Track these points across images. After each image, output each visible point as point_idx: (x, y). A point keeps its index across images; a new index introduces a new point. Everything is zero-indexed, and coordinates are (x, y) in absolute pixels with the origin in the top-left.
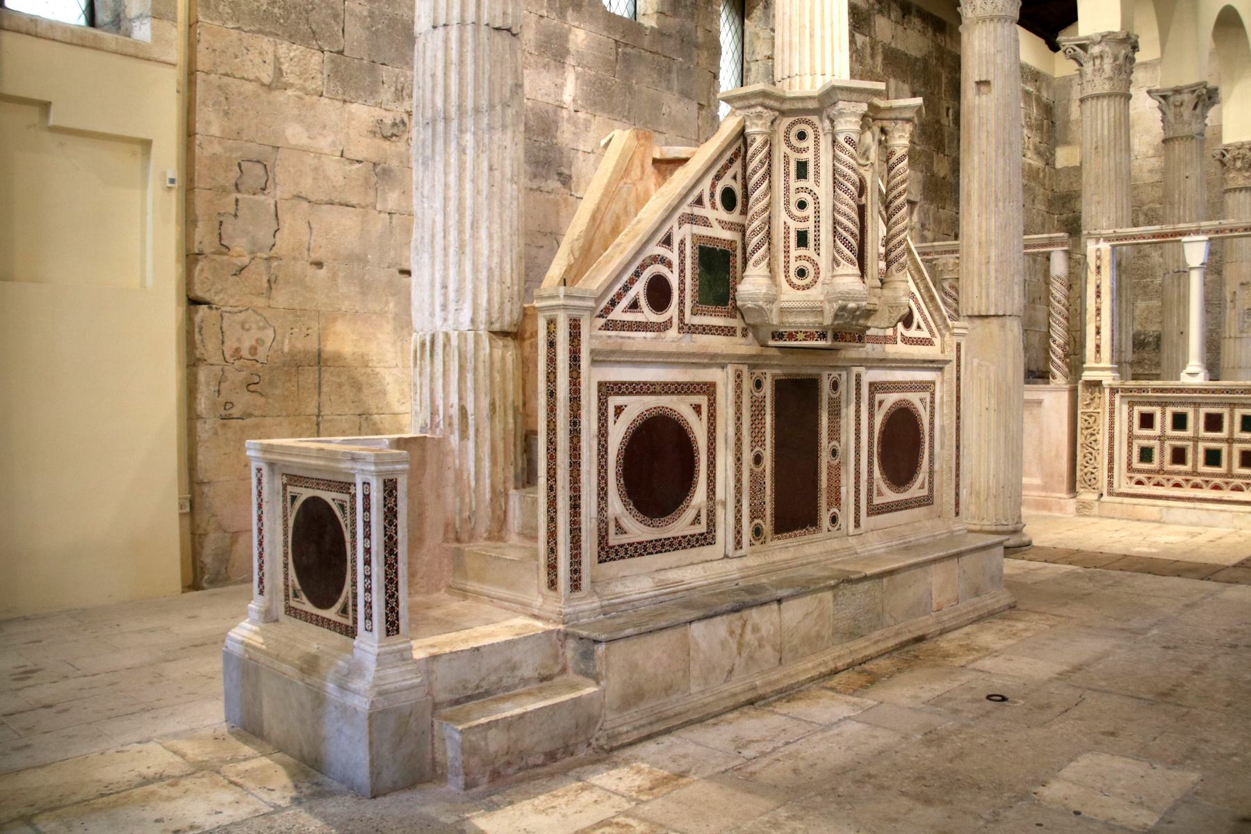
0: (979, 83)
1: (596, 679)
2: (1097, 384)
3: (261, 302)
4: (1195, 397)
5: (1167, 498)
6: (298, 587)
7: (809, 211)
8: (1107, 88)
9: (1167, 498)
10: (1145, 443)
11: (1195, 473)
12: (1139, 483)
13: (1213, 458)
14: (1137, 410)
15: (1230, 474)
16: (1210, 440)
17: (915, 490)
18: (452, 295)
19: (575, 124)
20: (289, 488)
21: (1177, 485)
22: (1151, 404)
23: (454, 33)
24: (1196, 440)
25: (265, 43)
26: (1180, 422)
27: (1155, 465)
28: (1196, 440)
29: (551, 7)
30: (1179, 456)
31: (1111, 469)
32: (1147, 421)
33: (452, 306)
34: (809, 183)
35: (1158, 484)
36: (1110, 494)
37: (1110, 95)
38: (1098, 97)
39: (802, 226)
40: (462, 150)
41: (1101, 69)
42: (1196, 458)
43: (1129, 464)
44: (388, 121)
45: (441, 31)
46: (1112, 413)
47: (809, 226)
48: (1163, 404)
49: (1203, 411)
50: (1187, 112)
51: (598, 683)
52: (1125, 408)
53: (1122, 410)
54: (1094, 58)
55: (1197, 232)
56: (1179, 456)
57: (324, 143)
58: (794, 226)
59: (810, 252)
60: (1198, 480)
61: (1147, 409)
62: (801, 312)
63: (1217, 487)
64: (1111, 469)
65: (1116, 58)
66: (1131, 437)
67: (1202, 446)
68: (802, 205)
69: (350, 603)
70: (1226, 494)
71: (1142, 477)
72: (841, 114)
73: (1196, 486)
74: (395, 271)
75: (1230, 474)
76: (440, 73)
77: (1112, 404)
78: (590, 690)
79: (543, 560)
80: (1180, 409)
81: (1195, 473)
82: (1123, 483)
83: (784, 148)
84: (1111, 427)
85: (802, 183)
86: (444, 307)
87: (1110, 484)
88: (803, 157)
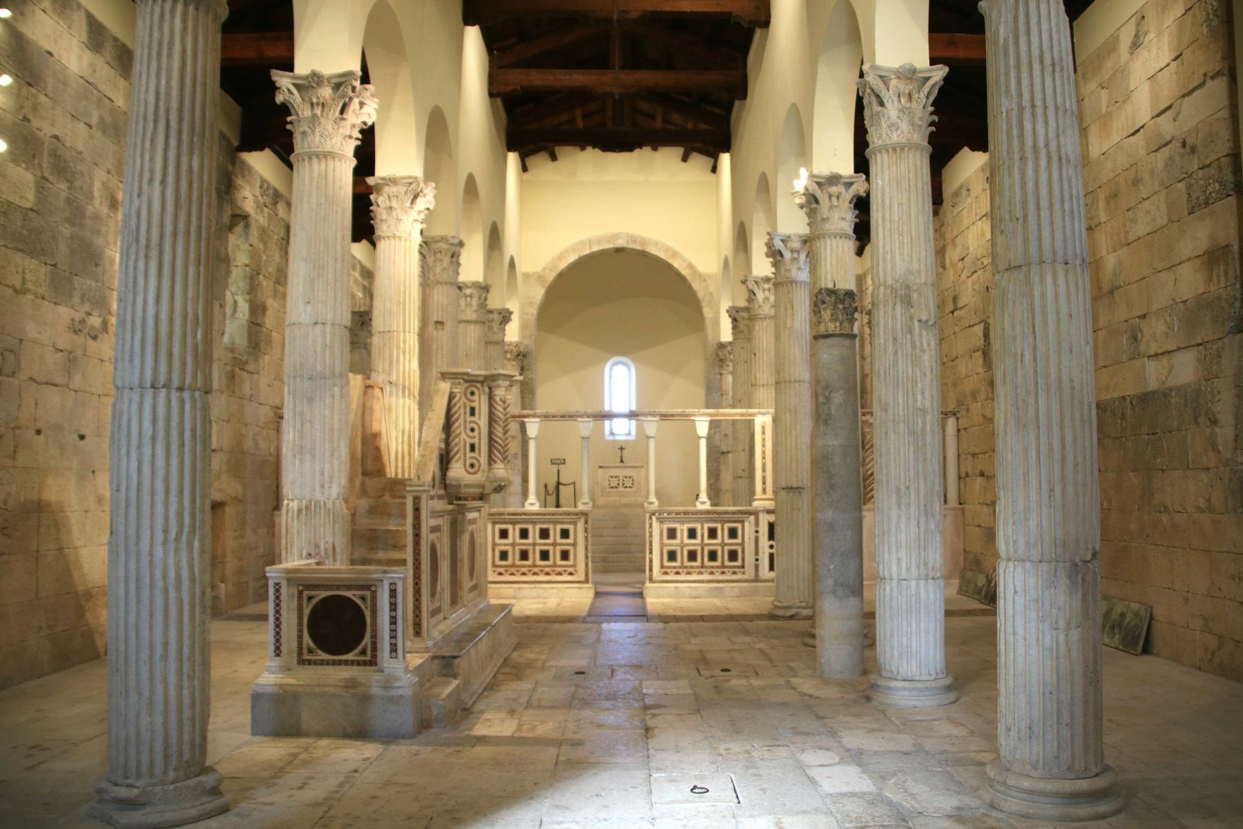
0: (438, 322)
1: (455, 676)
3: (10, 462)
4: (533, 518)
6: (312, 645)
7: (476, 433)
8: (474, 317)
10: (503, 548)
11: (534, 565)
12: (500, 574)
13: (545, 555)
14: (498, 527)
15: (555, 565)
16: (543, 544)
18: (327, 479)
21: (524, 574)
22: (506, 523)
23: (328, 329)
24: (534, 545)
25: (18, 257)
26: (524, 534)
27: (509, 562)
28: (534, 545)
30: (524, 555)
32: (504, 534)
33: (327, 486)
34: (476, 419)
35: (512, 574)
37: (476, 322)
38: (468, 322)
39: (472, 441)
40: (333, 397)
41: (471, 305)
42: (535, 556)
43: (493, 562)
44: (77, 320)
45: (319, 327)
47: (476, 441)
48: (514, 523)
49: (538, 527)
50: (496, 326)
51: (455, 678)
52: (489, 526)
54: (466, 296)
55: (534, 416)
56: (524, 555)
57: (45, 337)
58: (469, 441)
59: (476, 455)
60: (536, 570)
61: (503, 526)
63: (547, 574)
65: (480, 298)
66: (494, 545)
67: (538, 549)
68: (472, 430)
71: (501, 570)
73: (535, 574)
74: (76, 436)
75: (555, 565)
76: (319, 350)
80: (524, 526)
81: (534, 565)
83: (464, 399)
85: (472, 419)
86: (322, 486)
88: (474, 404)
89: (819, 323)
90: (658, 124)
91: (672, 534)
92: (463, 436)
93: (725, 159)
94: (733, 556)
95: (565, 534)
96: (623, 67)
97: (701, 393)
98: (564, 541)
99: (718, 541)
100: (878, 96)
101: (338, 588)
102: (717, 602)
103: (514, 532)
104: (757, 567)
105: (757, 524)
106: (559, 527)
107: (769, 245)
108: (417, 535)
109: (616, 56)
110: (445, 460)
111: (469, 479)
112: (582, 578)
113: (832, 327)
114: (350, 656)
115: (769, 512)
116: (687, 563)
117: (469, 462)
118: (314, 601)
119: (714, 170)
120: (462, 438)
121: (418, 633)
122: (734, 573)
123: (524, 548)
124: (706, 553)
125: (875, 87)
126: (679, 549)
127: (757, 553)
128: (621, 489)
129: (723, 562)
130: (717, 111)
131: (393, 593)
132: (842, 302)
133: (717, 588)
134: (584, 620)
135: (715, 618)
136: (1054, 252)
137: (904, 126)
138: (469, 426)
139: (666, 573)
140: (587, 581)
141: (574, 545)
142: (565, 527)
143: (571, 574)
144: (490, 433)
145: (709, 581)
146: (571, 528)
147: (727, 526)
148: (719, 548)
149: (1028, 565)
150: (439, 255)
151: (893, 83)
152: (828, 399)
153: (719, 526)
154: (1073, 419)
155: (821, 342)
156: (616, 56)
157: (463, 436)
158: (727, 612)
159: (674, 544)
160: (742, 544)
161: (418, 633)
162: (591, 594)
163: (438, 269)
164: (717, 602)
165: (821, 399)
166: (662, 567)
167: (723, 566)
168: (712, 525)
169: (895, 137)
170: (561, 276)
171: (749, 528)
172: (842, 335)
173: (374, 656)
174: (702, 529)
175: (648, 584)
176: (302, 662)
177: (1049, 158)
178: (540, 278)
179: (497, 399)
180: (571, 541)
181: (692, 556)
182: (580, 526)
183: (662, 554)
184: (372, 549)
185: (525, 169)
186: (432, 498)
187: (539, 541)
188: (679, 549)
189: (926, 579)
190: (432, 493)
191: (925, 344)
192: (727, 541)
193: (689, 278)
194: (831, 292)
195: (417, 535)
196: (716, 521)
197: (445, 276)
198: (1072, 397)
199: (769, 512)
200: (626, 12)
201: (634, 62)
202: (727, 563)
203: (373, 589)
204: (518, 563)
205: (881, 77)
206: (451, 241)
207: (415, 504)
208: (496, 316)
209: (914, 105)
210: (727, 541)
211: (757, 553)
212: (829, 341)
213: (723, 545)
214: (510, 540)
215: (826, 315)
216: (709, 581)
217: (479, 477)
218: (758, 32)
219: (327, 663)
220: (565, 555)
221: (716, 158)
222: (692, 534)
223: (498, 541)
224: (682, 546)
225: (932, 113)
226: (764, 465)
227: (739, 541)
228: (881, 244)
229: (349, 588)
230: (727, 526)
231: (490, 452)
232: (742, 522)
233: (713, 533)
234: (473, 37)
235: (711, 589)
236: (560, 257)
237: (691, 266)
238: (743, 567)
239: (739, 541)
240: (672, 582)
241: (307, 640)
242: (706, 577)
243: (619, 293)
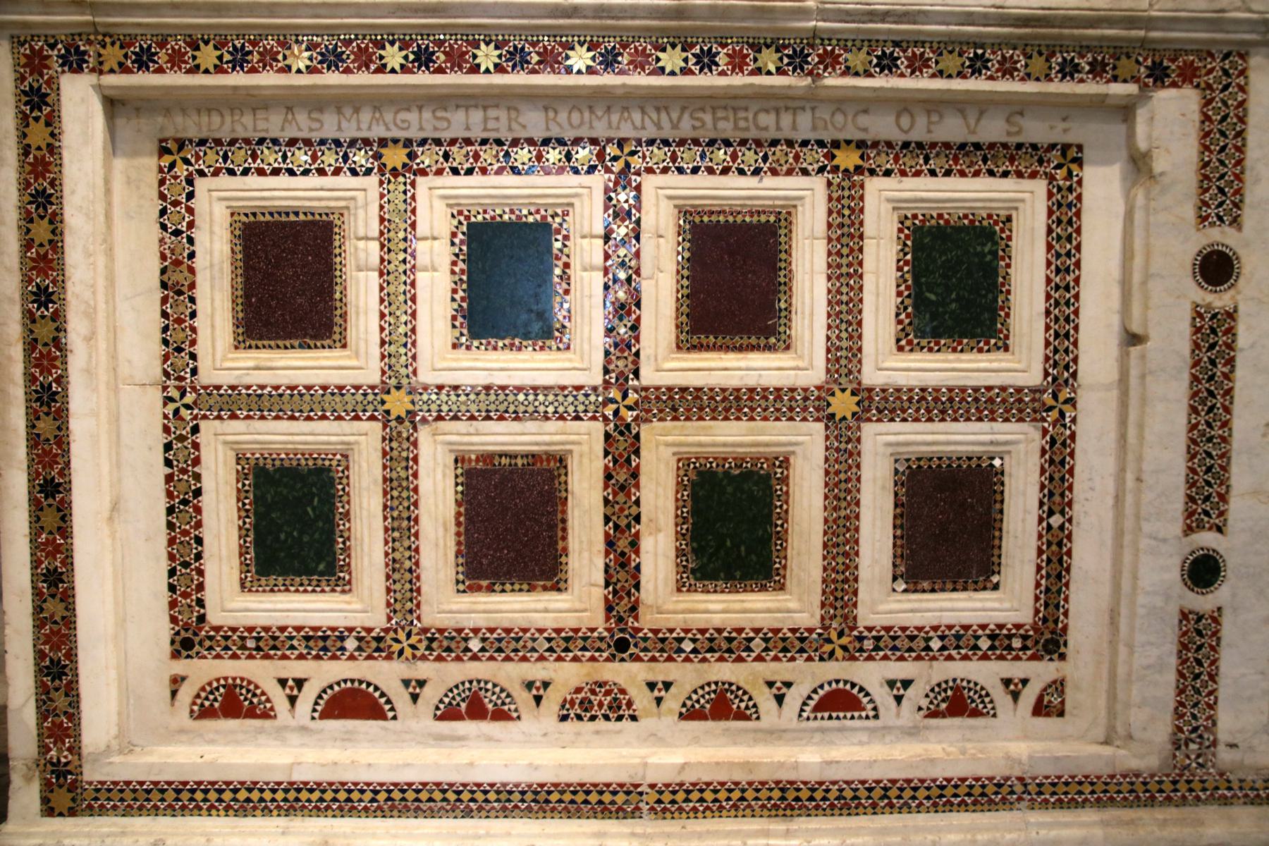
94: (949, 522)
116: (446, 602)
122: (958, 703)
124: (659, 497)
129: (840, 586)
139: (232, 703)
147: (886, 200)
148: (806, 444)
160: (1049, 404)
166: (187, 642)
167: (840, 631)
174: (624, 242)
181: (511, 522)
183: (183, 501)
188: (363, 443)
192: (887, 363)
196: (775, 153)
202: (883, 602)
210: (887, 363)
227: (1019, 363)
232: (1060, 164)
238: (1047, 637)
239: (1019, 363)
242: (663, 749)
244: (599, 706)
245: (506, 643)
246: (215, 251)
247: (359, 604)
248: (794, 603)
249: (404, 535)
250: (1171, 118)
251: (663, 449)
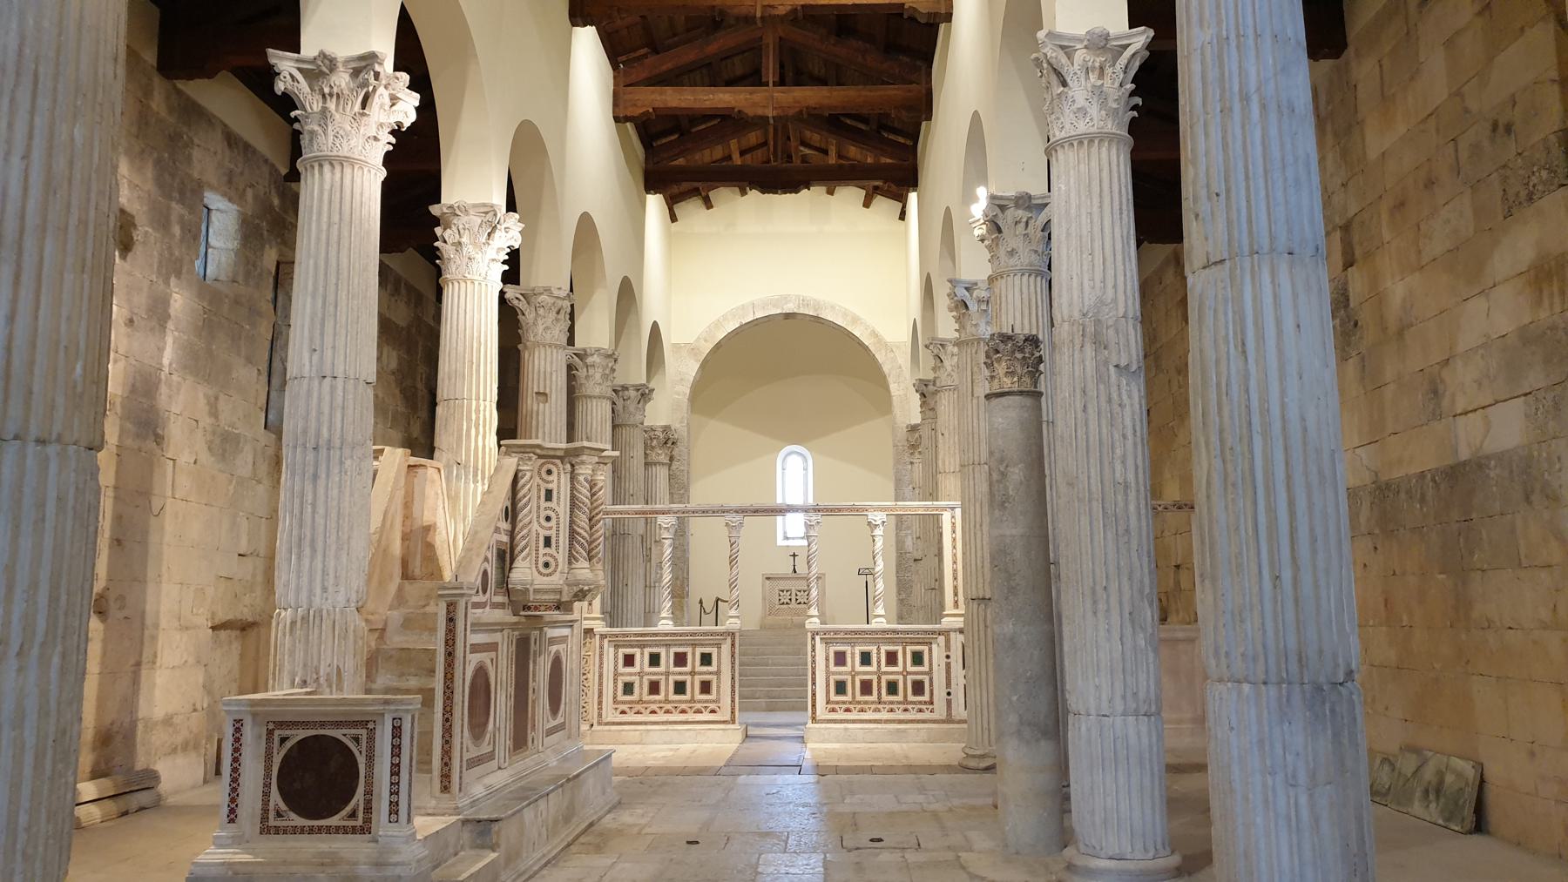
2: (589, 632)
4: (668, 640)
5: (646, 723)
7: (553, 523)
9: (646, 723)
10: (628, 679)
11: (667, 701)
12: (623, 712)
13: (680, 688)
14: (622, 651)
15: (693, 700)
17: (560, 720)
19: (170, 387)
20: (277, 733)
21: (653, 712)
26: (655, 660)
27: (635, 697)
28: (667, 674)
29: (159, 273)
30: (654, 688)
31: (600, 703)
32: (629, 660)
34: (553, 504)
36: (599, 724)
39: (548, 533)
42: (667, 688)
46: (601, 655)
47: (553, 533)
48: (642, 646)
49: (673, 650)
52: (612, 650)
53: (610, 651)
56: (654, 688)
58: (543, 533)
59: (552, 551)
60: (669, 706)
61: (629, 651)
62: (546, 592)
63: (683, 712)
64: (600, 703)
66: (616, 674)
67: (672, 679)
68: (548, 519)
69: (361, 808)
70: (690, 716)
71: (625, 707)
72: (583, 463)
73: (667, 712)
75: (693, 700)
77: (601, 647)
78: (493, 855)
79: (436, 772)
80: (655, 650)
81: (667, 701)
82: (610, 714)
83: (537, 479)
84: (601, 667)
85: (548, 504)
86: (325, 589)
87: (600, 715)
88: (550, 486)
89: (992, 377)
90: (832, 159)
91: (840, 659)
92: (535, 526)
93: (913, 197)
94: (918, 688)
95: (706, 659)
96: (781, 82)
97: (891, 487)
98: (705, 669)
99: (899, 668)
100: (1059, 74)
101: (323, 724)
102: (896, 747)
103: (642, 658)
104: (949, 703)
105: (948, 647)
106: (699, 651)
107: (952, 295)
108: (450, 655)
109: (770, 71)
110: (506, 557)
111: (541, 582)
112: (728, 717)
113: (1008, 383)
114: (334, 821)
115: (961, 631)
116: (859, 698)
117: (541, 560)
118: (289, 744)
119: (902, 216)
120: (532, 525)
121: (445, 789)
122: (920, 711)
123: (654, 678)
124: (884, 685)
125: (1053, 61)
126: (849, 678)
127: (948, 684)
128: (793, 605)
129: (905, 696)
130: (901, 140)
131: (397, 732)
132: (1021, 350)
133: (898, 730)
134: (717, 772)
135: (888, 770)
136: (1272, 238)
137: (1094, 110)
138: (543, 514)
139: (833, 710)
140: (733, 722)
141: (718, 673)
142: (707, 650)
143: (713, 711)
144: (572, 522)
145: (887, 721)
146: (714, 651)
147: (909, 649)
149: (1246, 687)
150: (541, 311)
151: (1080, 55)
152: (1003, 475)
153: (899, 649)
154: (1306, 474)
155: (995, 401)
156: (770, 71)
157: (535, 526)
158: (905, 762)
159: (842, 672)
160: (930, 673)
161: (445, 789)
162: (739, 736)
163: (540, 328)
164: (896, 747)
165: (995, 476)
167: (905, 701)
168: (891, 648)
169: (1082, 127)
170: (718, 346)
171: (938, 651)
172: (1021, 393)
173: (367, 820)
174: (879, 653)
175: (810, 725)
176: (266, 830)
177: (1263, 107)
178: (693, 350)
179: (581, 478)
180: (713, 668)
181: (866, 688)
182: (726, 648)
183: (828, 685)
184: (402, 675)
185: (673, 218)
186: (477, 605)
187: (673, 669)
189: (1136, 714)
190: (481, 598)
191: (1125, 397)
192: (910, 668)
193: (872, 348)
194: (1005, 338)
195: (450, 655)
197: (548, 336)
198: (1305, 444)
199: (961, 631)
200: (772, 7)
201: (794, 73)
202: (911, 698)
203: (371, 726)
204: (646, 697)
205: (1062, 47)
206: (556, 293)
207: (448, 612)
208: (632, 393)
209: (1107, 82)
210: (910, 668)
211: (948, 684)
212: (1004, 400)
213: (905, 673)
214: (637, 669)
215: (1001, 368)
216: (887, 721)
217: (556, 580)
218: (942, 27)
219: (302, 830)
220: (706, 687)
221: (902, 199)
222: (866, 659)
223: (621, 669)
224: (854, 674)
225: (1132, 94)
226: (955, 571)
227: (925, 668)
228: (1064, 268)
229: (338, 724)
230: (909, 649)
231: (571, 546)
233: (892, 658)
234: (586, 41)
235: (890, 732)
236: (718, 324)
237: (874, 334)
239: (925, 668)
240: (841, 721)
241: (276, 798)
242: (885, 715)
243: (791, 362)
244: (877, 710)
245: (866, 703)
246: (832, 656)
247: (848, 698)
248: (900, 698)
249: (852, 689)
250: (942, 639)
251: (884, 678)
